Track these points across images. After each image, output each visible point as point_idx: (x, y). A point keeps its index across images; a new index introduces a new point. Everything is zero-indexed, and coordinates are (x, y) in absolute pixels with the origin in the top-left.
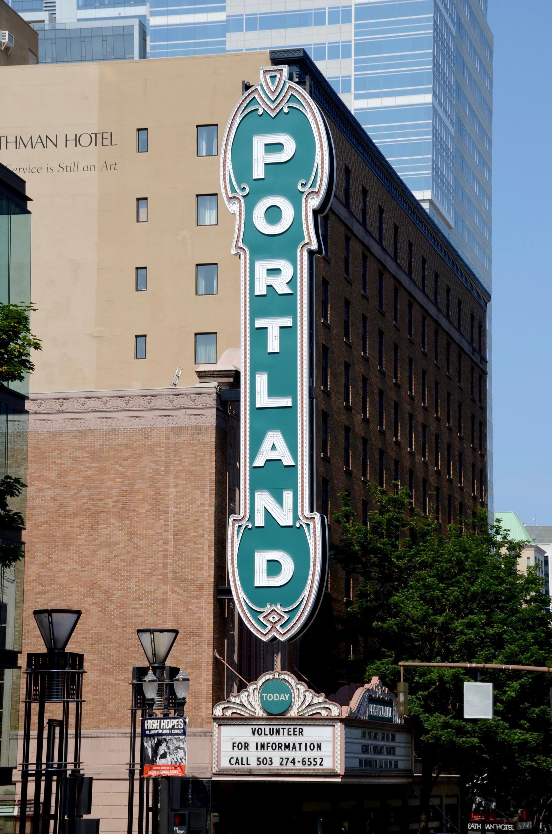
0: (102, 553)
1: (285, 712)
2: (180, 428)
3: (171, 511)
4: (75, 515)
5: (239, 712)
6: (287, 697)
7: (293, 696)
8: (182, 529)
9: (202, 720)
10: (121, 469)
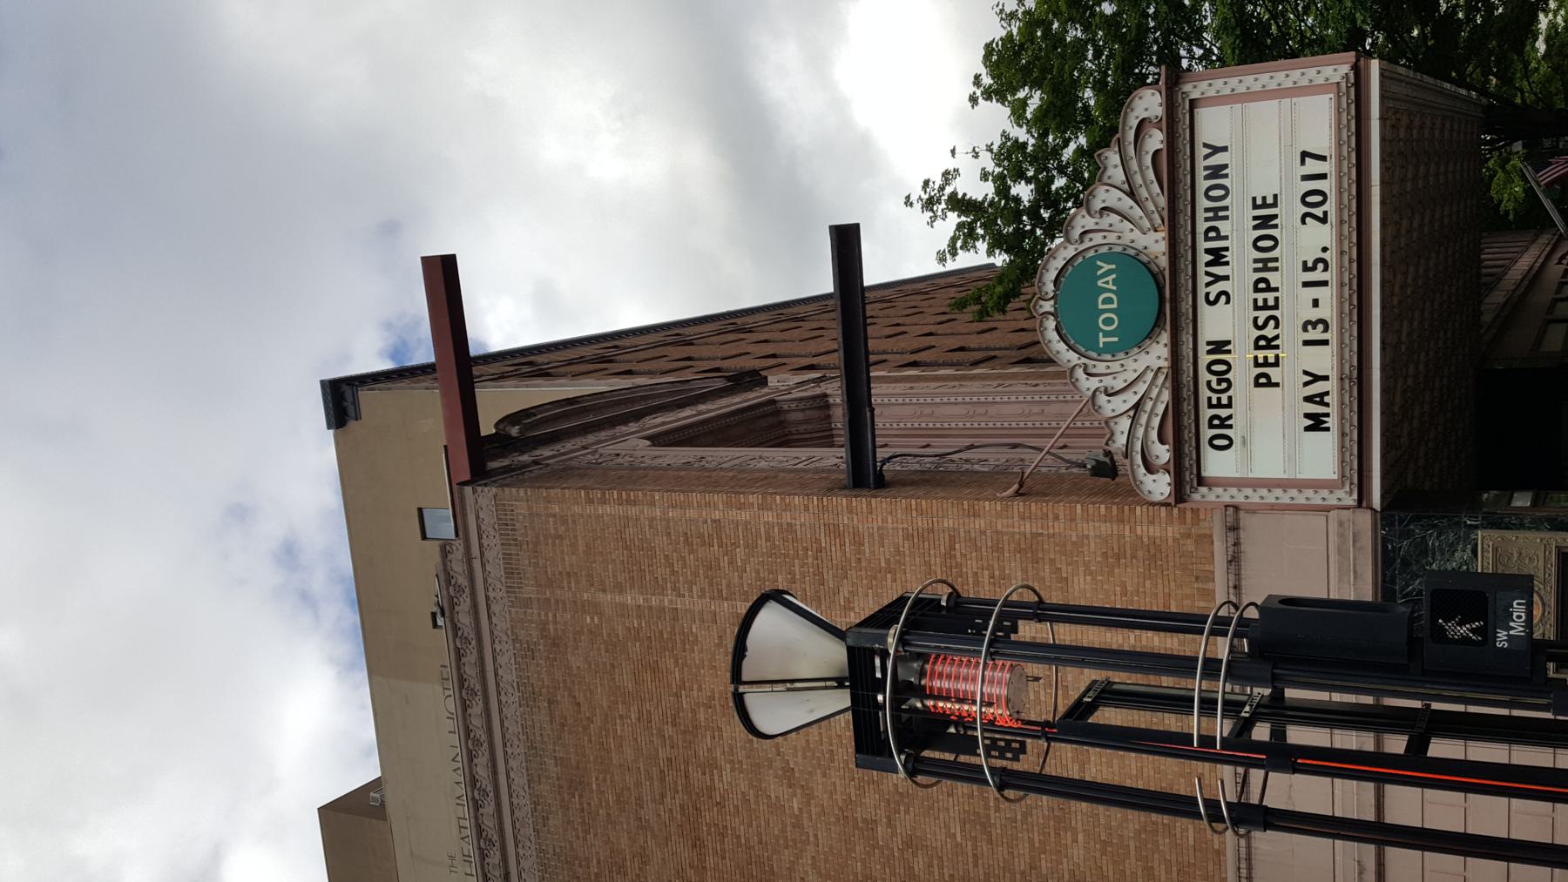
0: (775, 789)
1: (1154, 275)
2: (510, 573)
3: (671, 602)
4: (697, 844)
5: (1156, 422)
6: (1107, 267)
7: (1104, 250)
8: (706, 577)
9: (1189, 536)
10: (598, 720)
